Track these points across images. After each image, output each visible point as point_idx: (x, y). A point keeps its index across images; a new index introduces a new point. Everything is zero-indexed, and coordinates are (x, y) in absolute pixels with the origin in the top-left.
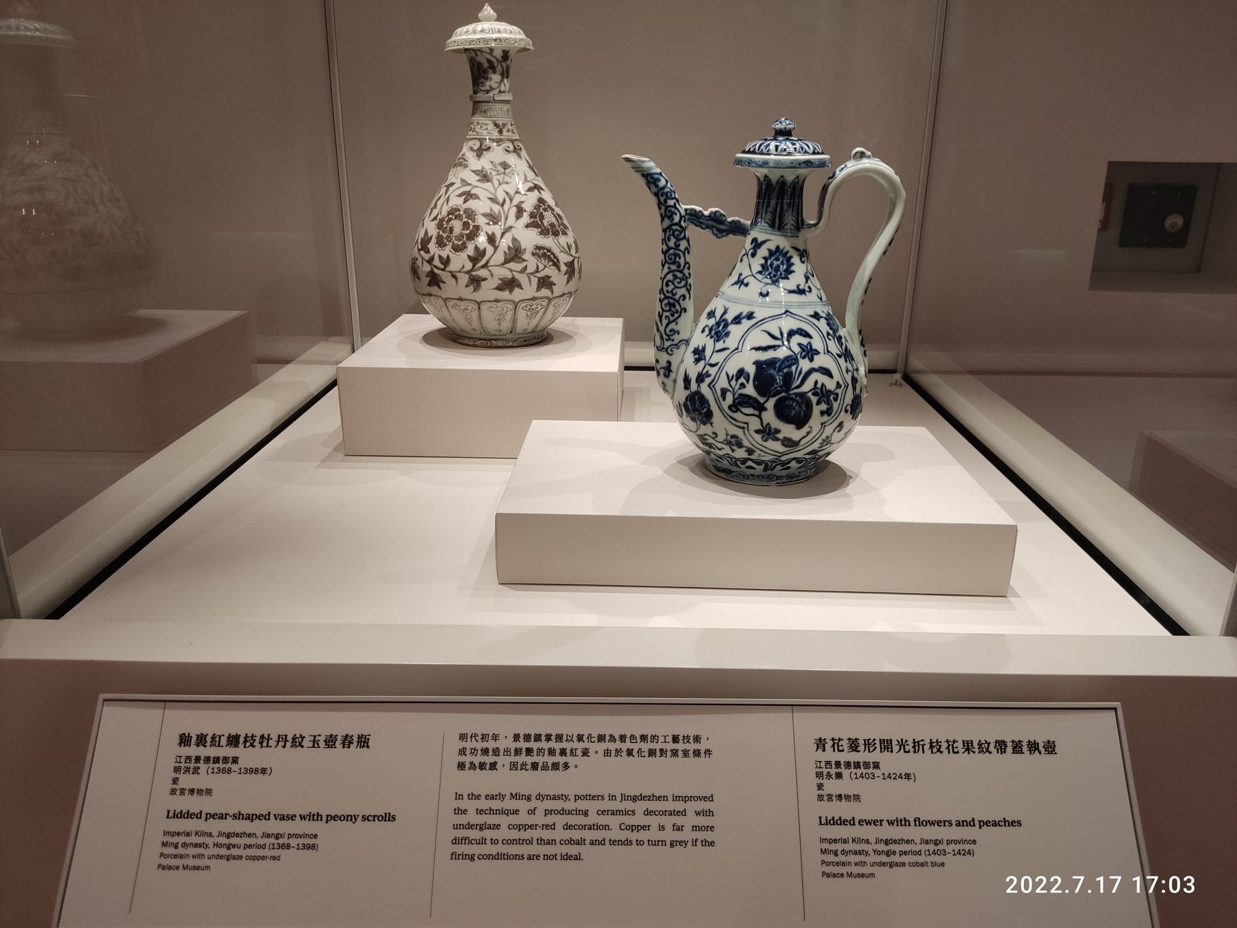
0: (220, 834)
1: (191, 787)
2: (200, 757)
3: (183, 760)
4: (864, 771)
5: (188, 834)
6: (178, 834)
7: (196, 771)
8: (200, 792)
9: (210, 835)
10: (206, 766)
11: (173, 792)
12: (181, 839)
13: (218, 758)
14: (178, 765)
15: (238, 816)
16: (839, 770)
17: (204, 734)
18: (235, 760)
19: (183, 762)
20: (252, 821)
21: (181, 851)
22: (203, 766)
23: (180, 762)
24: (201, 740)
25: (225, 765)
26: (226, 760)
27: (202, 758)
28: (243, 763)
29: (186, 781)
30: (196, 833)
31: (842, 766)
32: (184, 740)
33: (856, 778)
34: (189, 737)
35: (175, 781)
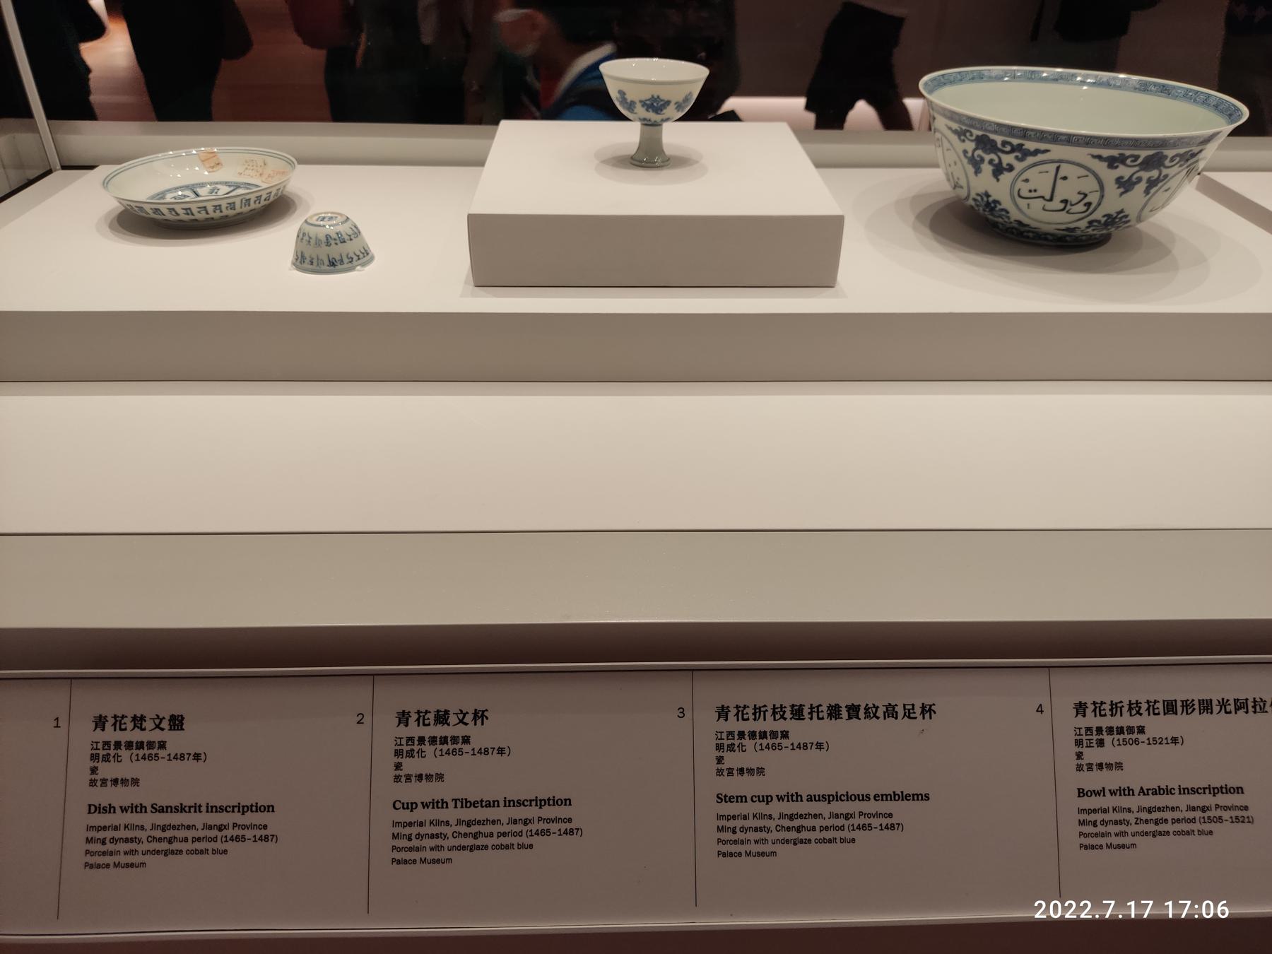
1: (418, 773)
2: (424, 737)
4: (771, 742)
9: (447, 823)
10: (433, 748)
13: (446, 738)
15: (211, 809)
16: (1101, 737)
18: (466, 740)
19: (725, 738)
20: (243, 814)
23: (401, 745)
24: (422, 718)
27: (427, 739)
28: (476, 743)
31: (1104, 733)
33: (762, 749)
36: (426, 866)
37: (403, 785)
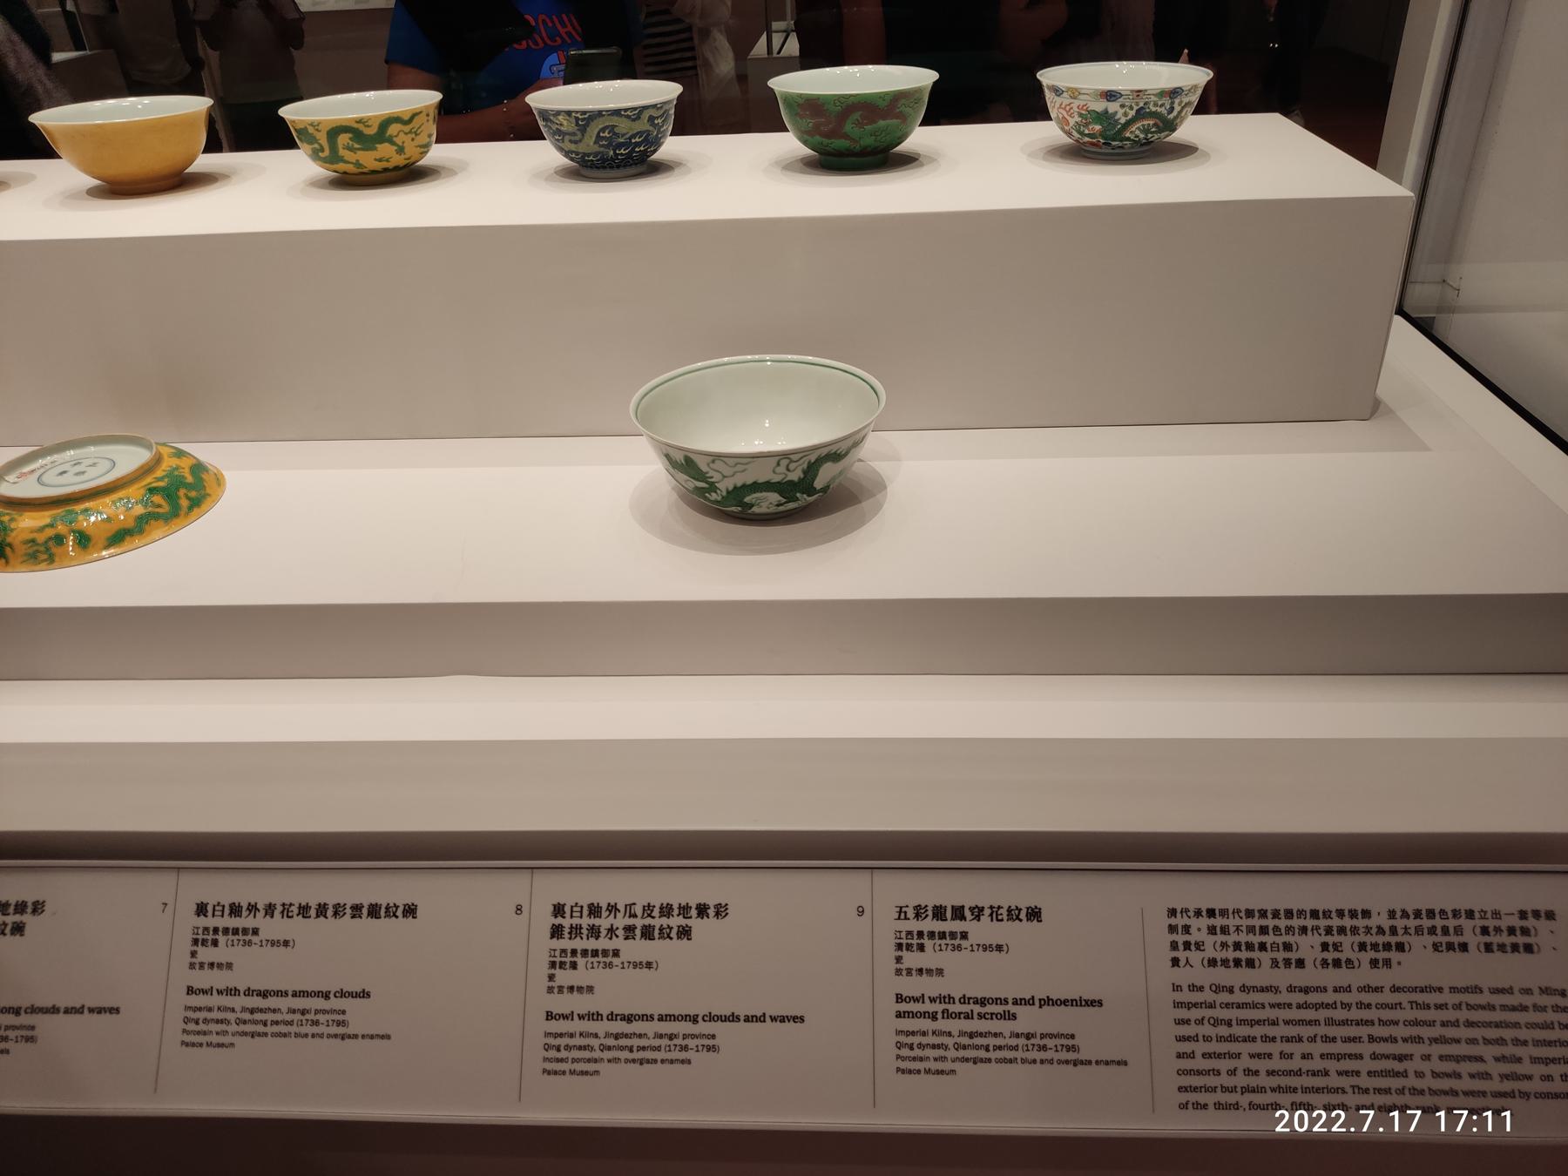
0: (244, 1010)
3: (200, 931)
5: (210, 1010)
6: (200, 1009)
7: (215, 943)
8: (220, 966)
9: (233, 1010)
11: (192, 966)
12: (201, 1015)
13: (238, 929)
14: (195, 937)
17: (205, 902)
21: (202, 1027)
22: (221, 938)
23: (197, 934)
25: (245, 937)
26: (245, 931)
27: (221, 929)
29: (205, 954)
30: (219, 1009)
32: (201, 909)
34: (240, 906)
35: (193, 954)
36: (211, 1049)
37: (197, 972)
